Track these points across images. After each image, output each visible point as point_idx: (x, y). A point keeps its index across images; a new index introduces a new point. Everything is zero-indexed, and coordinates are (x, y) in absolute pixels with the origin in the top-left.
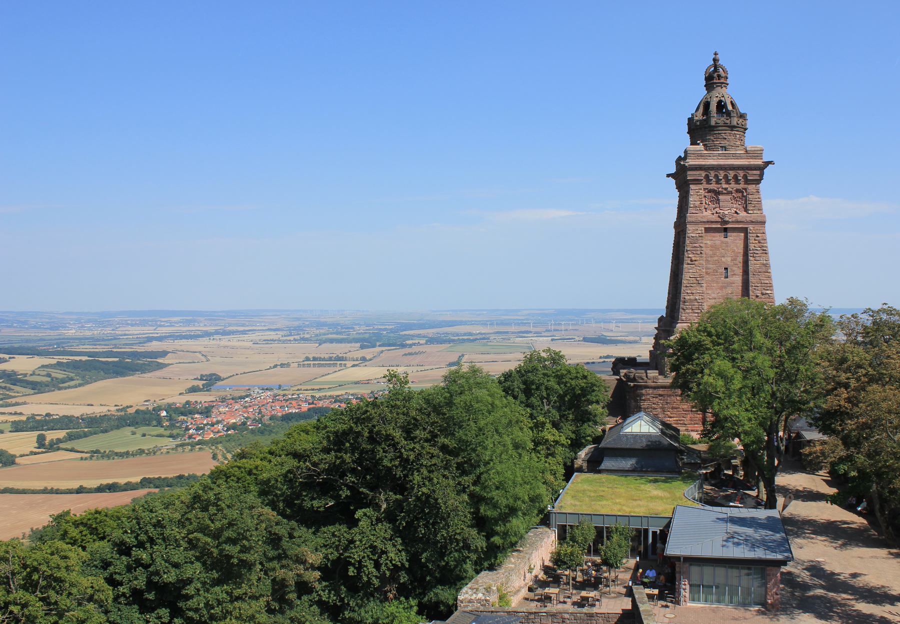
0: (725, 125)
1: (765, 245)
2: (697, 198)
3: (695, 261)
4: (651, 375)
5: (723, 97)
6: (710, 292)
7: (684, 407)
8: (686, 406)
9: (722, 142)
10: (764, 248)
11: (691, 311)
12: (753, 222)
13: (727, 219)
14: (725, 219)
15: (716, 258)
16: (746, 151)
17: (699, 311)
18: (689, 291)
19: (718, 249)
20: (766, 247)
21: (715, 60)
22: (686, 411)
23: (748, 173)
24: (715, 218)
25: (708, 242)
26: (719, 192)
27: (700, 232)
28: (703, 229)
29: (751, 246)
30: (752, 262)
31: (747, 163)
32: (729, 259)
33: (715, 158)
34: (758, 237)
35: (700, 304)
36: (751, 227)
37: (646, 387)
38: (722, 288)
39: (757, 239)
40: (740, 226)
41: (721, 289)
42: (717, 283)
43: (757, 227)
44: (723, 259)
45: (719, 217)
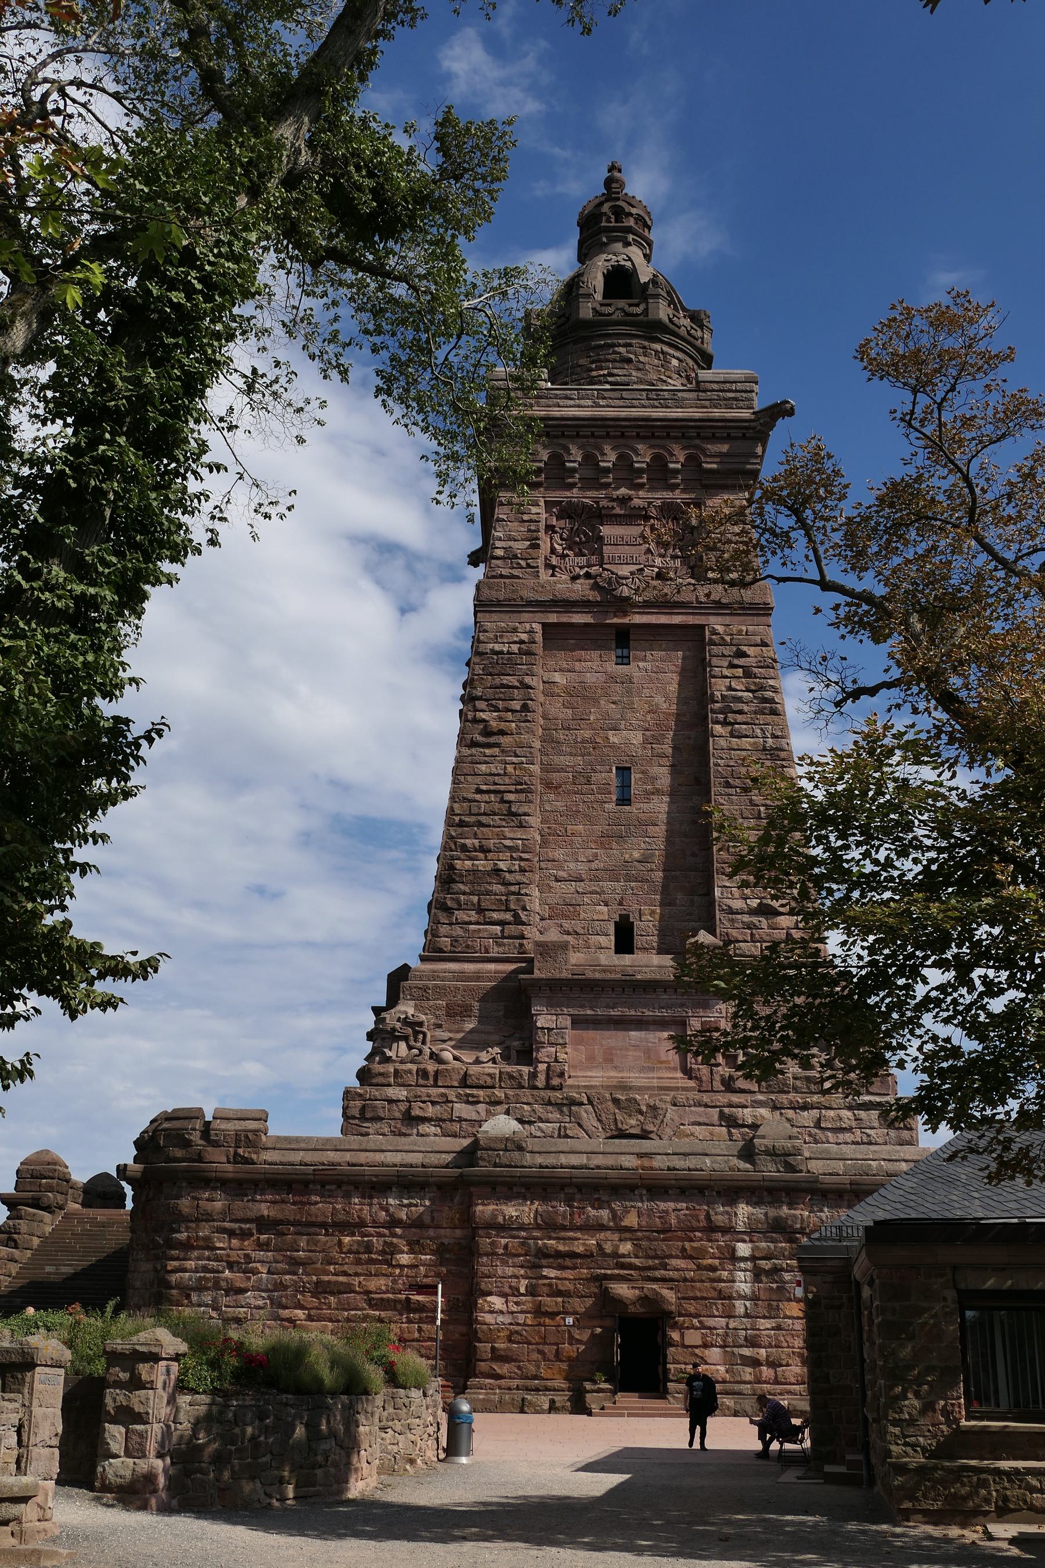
0: (630, 321)
1: (771, 682)
2: (516, 528)
3: (502, 733)
4: (223, 1127)
5: (630, 259)
6: (559, 854)
7: (373, 1284)
8: (382, 1282)
9: (615, 371)
10: (769, 694)
11: (473, 916)
12: (726, 606)
13: (626, 592)
14: (617, 593)
15: (587, 734)
16: (698, 383)
17: (508, 916)
18: (468, 842)
19: (596, 701)
20: (776, 690)
21: (609, 182)
22: (382, 1304)
23: (703, 451)
24: (581, 589)
25: (557, 677)
26: (600, 509)
27: (524, 637)
28: (537, 627)
29: (719, 687)
30: (723, 743)
31: (698, 415)
32: (637, 738)
33: (589, 403)
34: (744, 655)
35: (513, 888)
36: (717, 624)
37: (202, 1181)
38: (605, 840)
39: (736, 662)
40: (677, 620)
41: (602, 846)
42: (590, 820)
43: (741, 625)
44: (614, 738)
45: (596, 587)
